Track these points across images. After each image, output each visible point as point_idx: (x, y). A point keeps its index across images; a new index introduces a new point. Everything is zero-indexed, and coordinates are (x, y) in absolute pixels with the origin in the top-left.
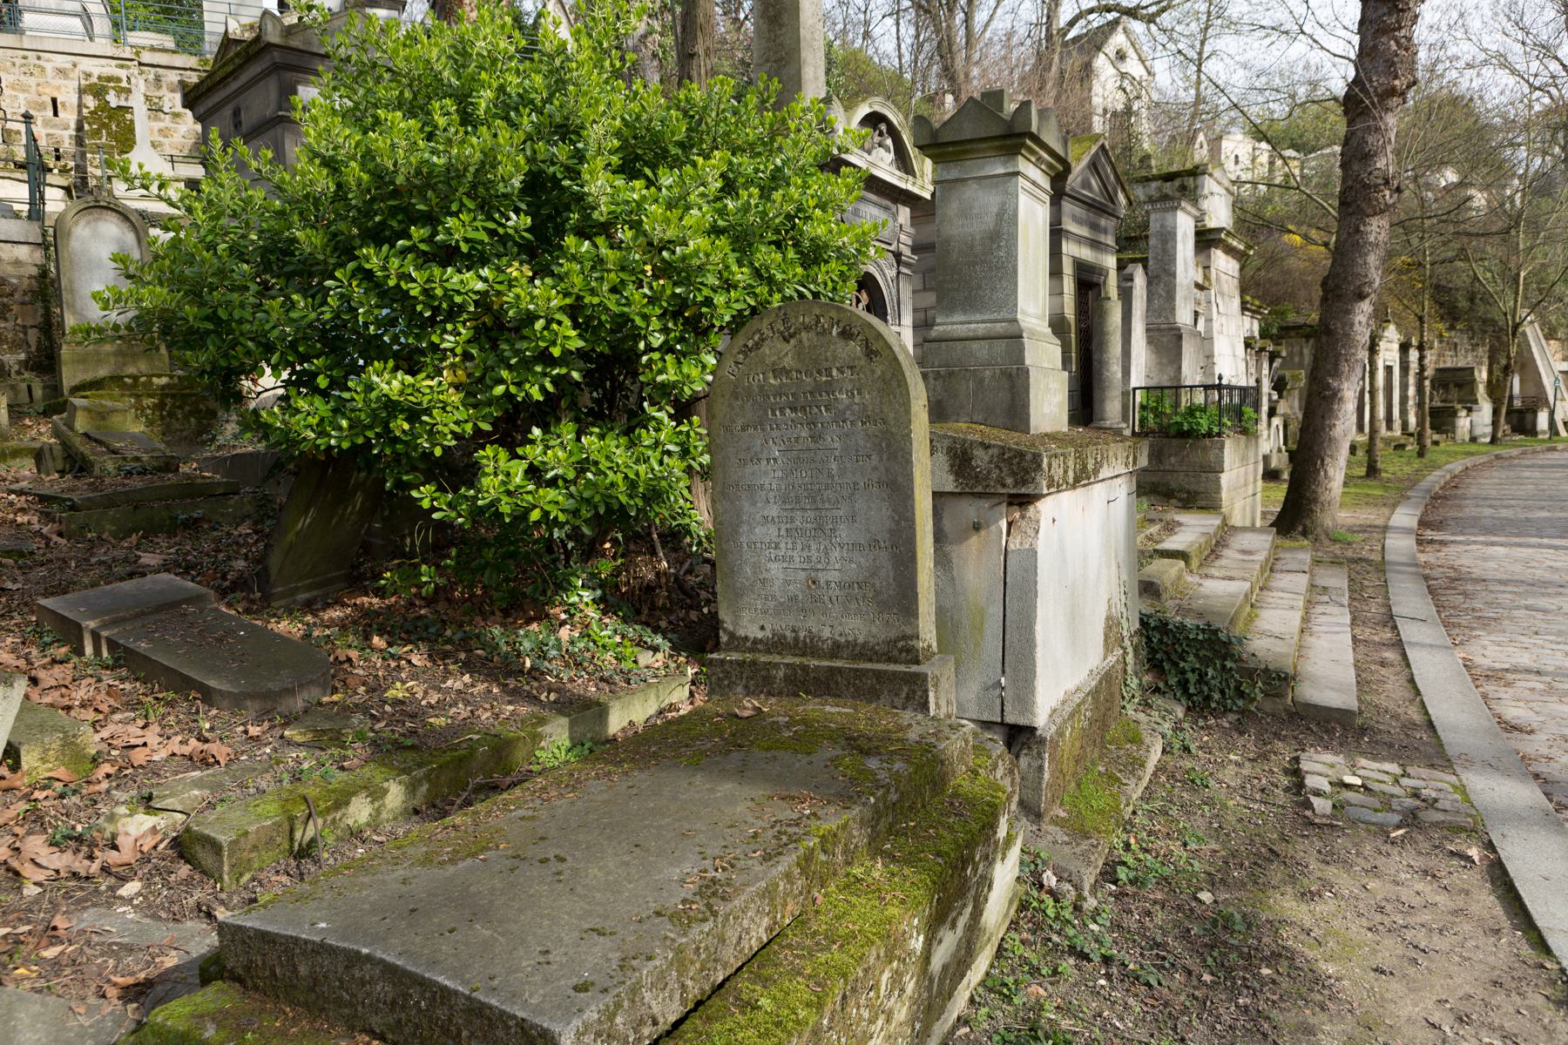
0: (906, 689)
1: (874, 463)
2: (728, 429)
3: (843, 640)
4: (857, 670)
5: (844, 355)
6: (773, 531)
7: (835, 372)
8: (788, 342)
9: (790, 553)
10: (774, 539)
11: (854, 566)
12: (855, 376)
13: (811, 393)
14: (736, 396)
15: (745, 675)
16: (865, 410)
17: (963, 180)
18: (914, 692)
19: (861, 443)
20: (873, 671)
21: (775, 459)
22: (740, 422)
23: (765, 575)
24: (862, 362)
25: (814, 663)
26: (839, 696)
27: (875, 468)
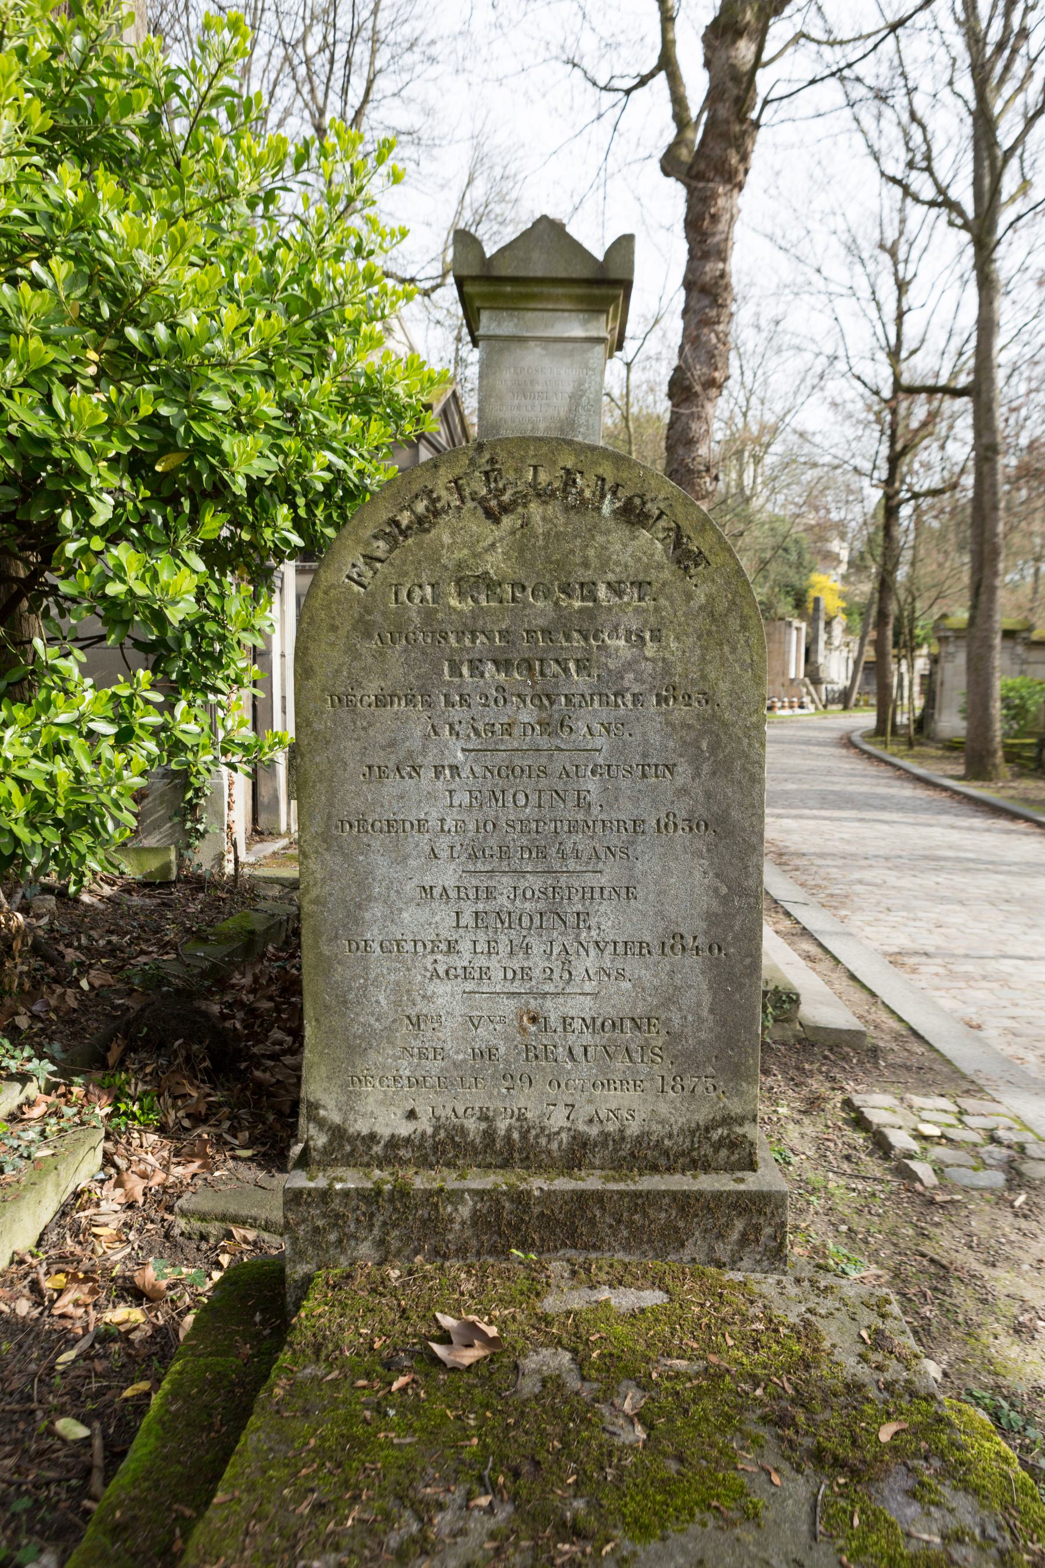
0: (739, 1225)
1: (680, 781)
2: (343, 700)
3: (594, 1131)
4: (637, 1194)
5: (626, 558)
6: (443, 917)
7: (602, 592)
8: (497, 521)
9: (482, 961)
10: (445, 934)
11: (626, 985)
12: (648, 603)
13: (547, 632)
14: (365, 628)
15: (379, 1219)
16: (667, 671)
17: (522, 340)
18: (758, 1229)
19: (655, 739)
20: (674, 1195)
21: (455, 769)
22: (373, 687)
23: (422, 1007)
24: (666, 575)
25: (537, 1184)
26: (595, 1248)
27: (684, 791)
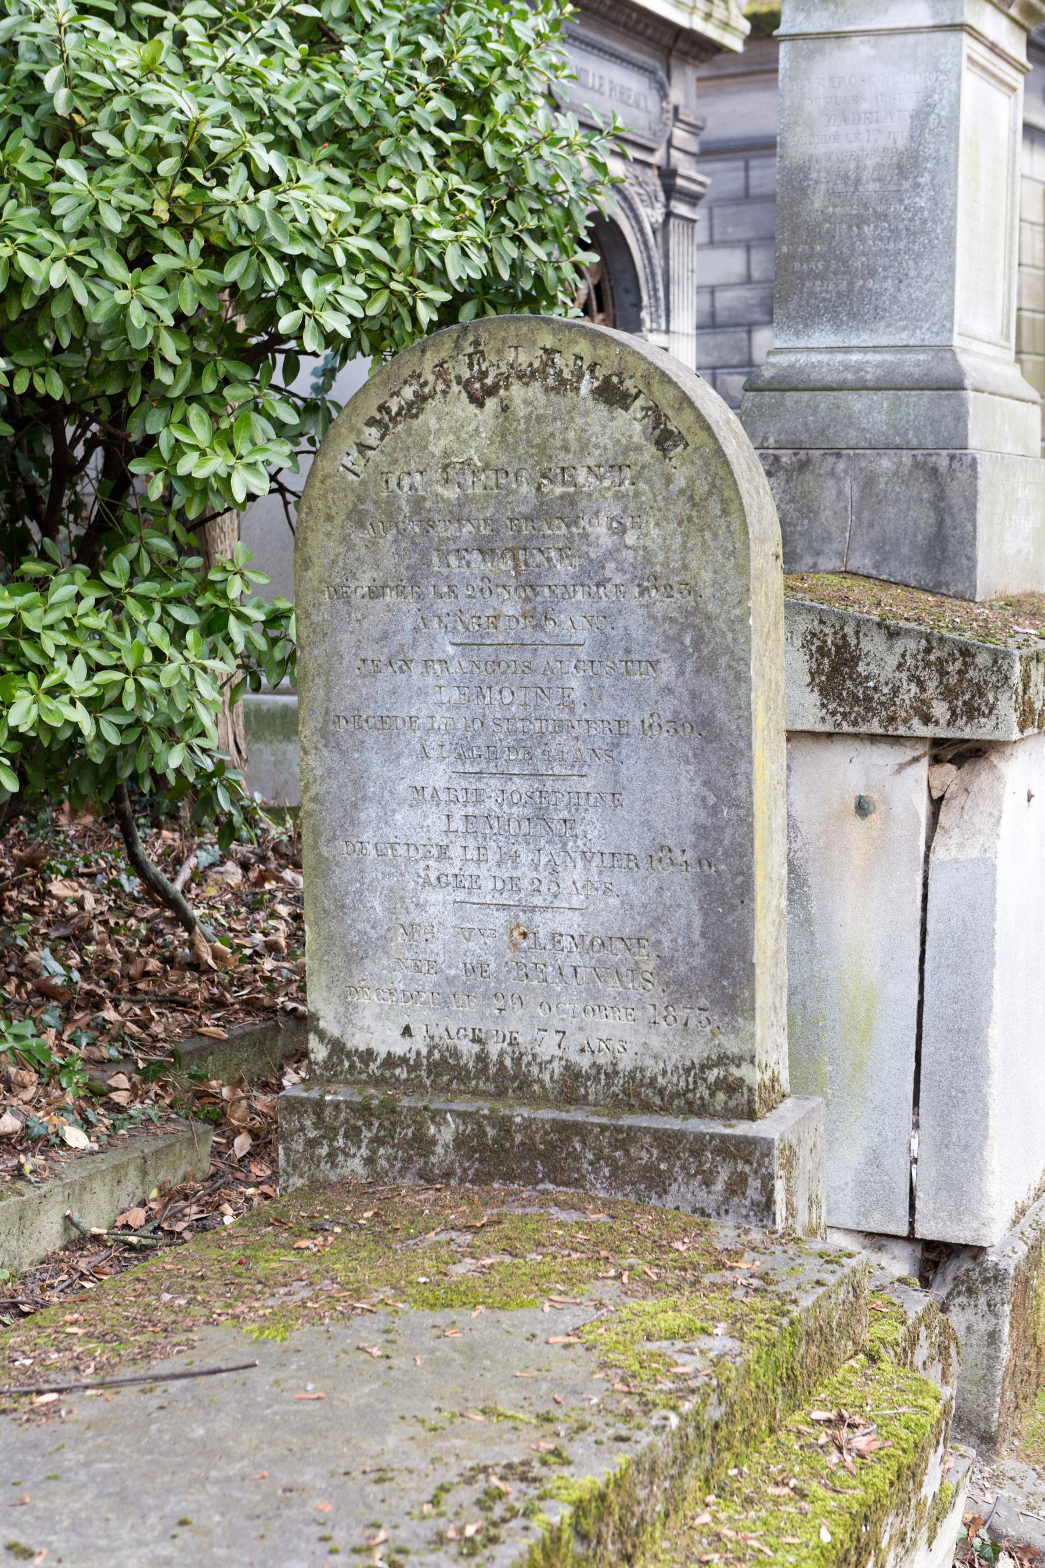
1: (664, 679)
2: (340, 593)
3: (584, 1062)
5: (604, 441)
6: (434, 820)
7: (582, 477)
8: (481, 405)
9: (471, 869)
10: (437, 839)
14: (358, 518)
16: (648, 561)
19: (638, 634)
22: (365, 579)
23: (415, 916)
25: (520, 1114)
27: (668, 690)
